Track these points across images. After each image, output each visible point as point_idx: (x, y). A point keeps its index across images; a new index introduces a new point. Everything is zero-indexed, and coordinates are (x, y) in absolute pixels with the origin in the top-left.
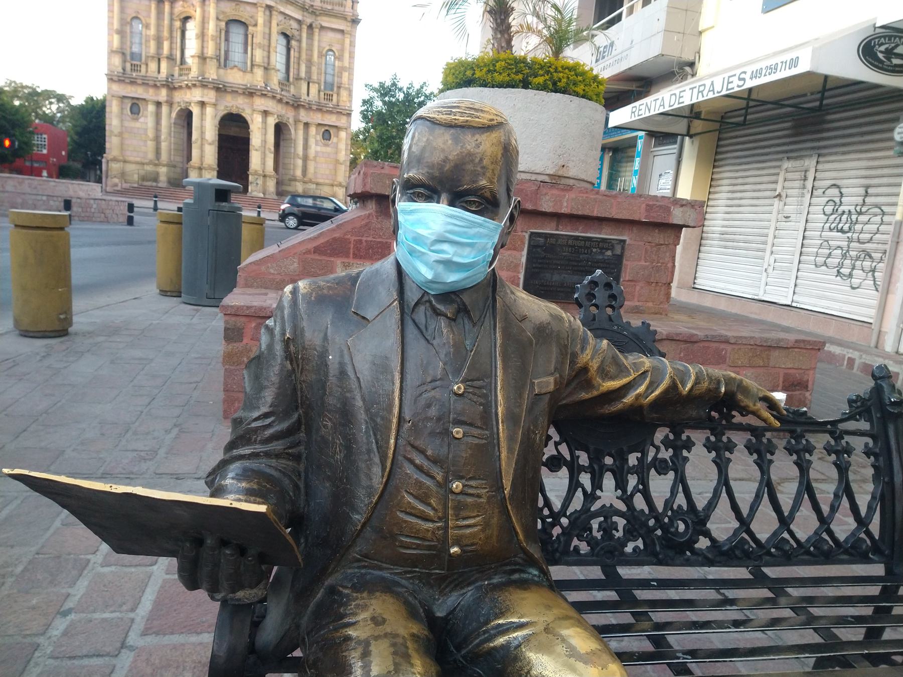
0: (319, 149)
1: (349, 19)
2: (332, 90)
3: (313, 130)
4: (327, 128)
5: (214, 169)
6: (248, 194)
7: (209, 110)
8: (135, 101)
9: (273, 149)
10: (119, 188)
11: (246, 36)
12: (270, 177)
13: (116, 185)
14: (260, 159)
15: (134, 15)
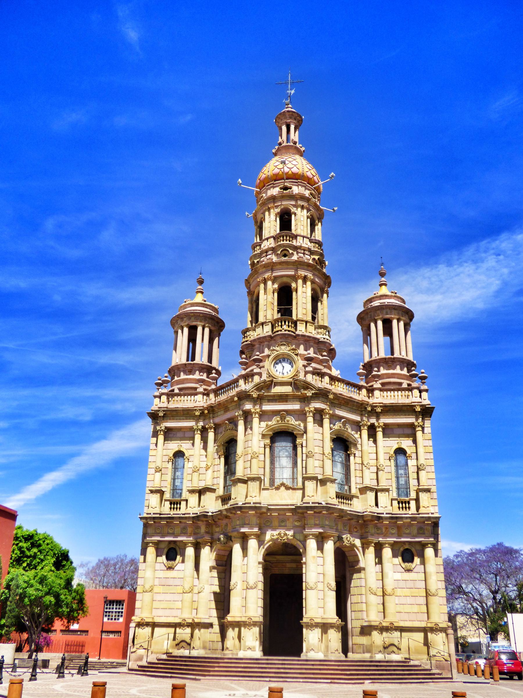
0: (398, 576)
1: (418, 409)
2: (407, 494)
3: (387, 552)
4: (407, 547)
5: (255, 624)
6: (303, 656)
7: (253, 543)
8: (172, 546)
9: (333, 584)
10: (144, 663)
11: (295, 448)
12: (332, 626)
13: (140, 659)
14: (318, 601)
15: (177, 449)
